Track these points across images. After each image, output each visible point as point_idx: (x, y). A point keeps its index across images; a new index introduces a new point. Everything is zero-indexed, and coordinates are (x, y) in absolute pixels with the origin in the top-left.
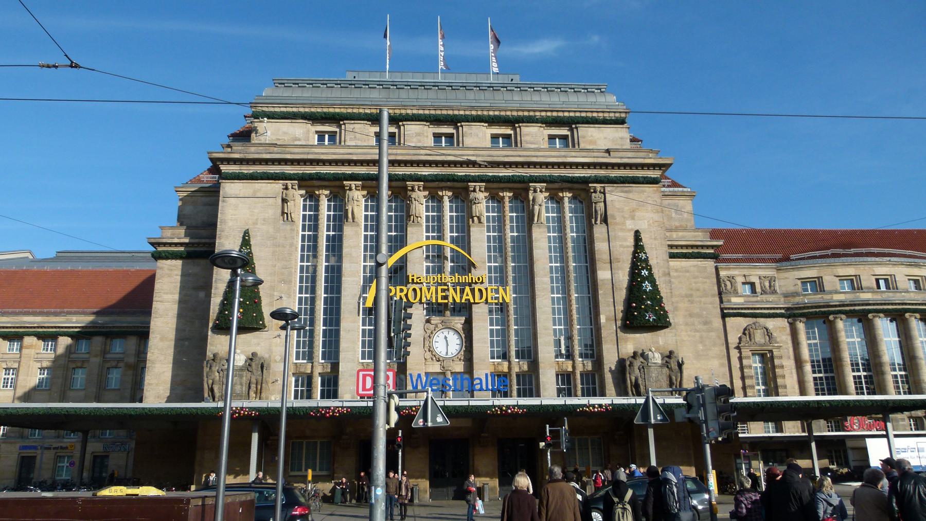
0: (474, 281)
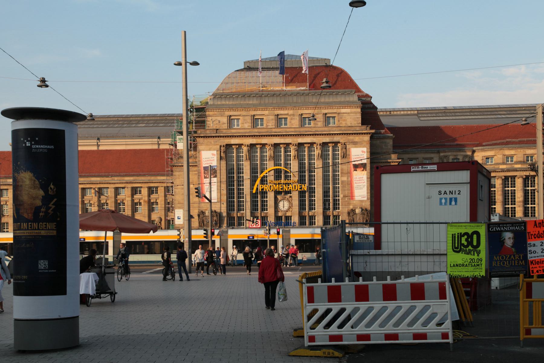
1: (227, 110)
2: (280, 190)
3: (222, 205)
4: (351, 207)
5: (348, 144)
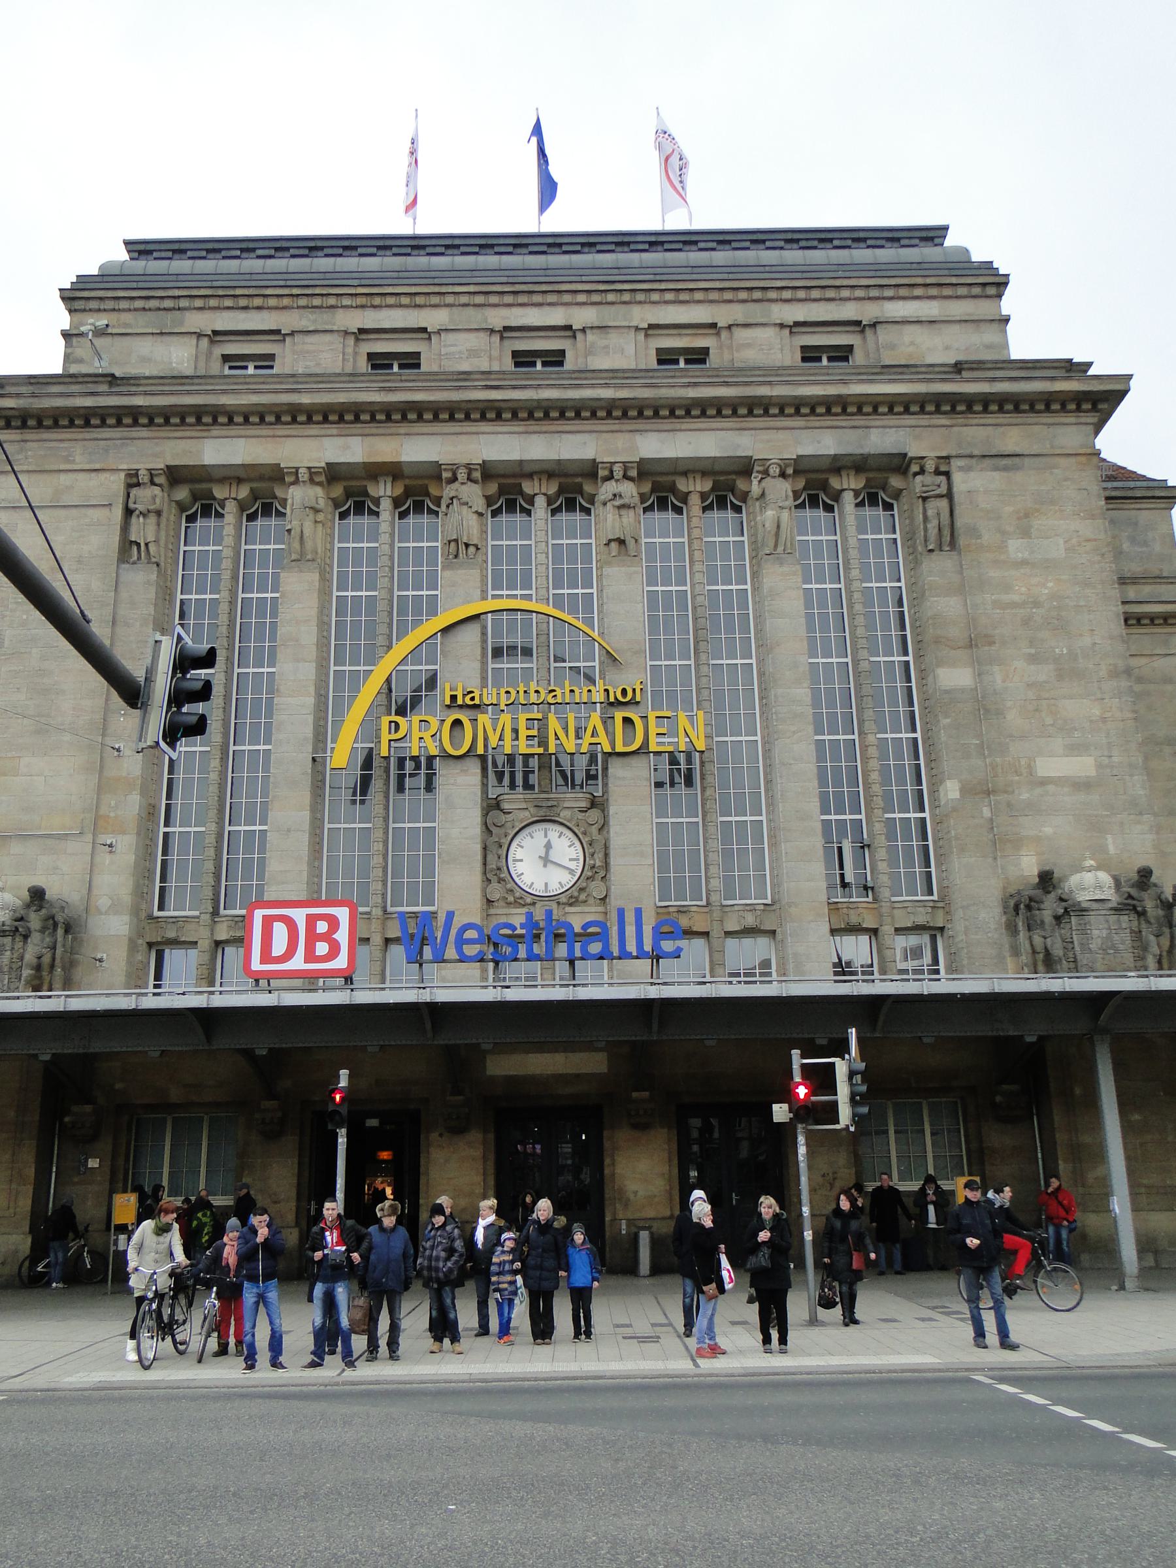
0: (612, 699)
1: (199, 303)
3: (104, 858)
4: (1028, 866)
5: (961, 469)
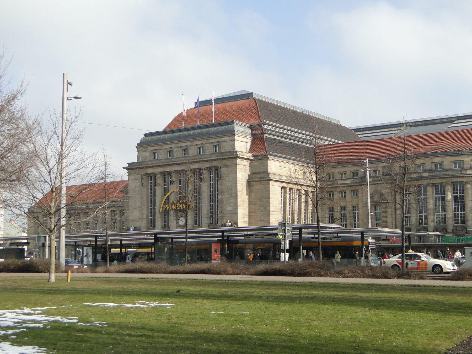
2: (177, 209)
